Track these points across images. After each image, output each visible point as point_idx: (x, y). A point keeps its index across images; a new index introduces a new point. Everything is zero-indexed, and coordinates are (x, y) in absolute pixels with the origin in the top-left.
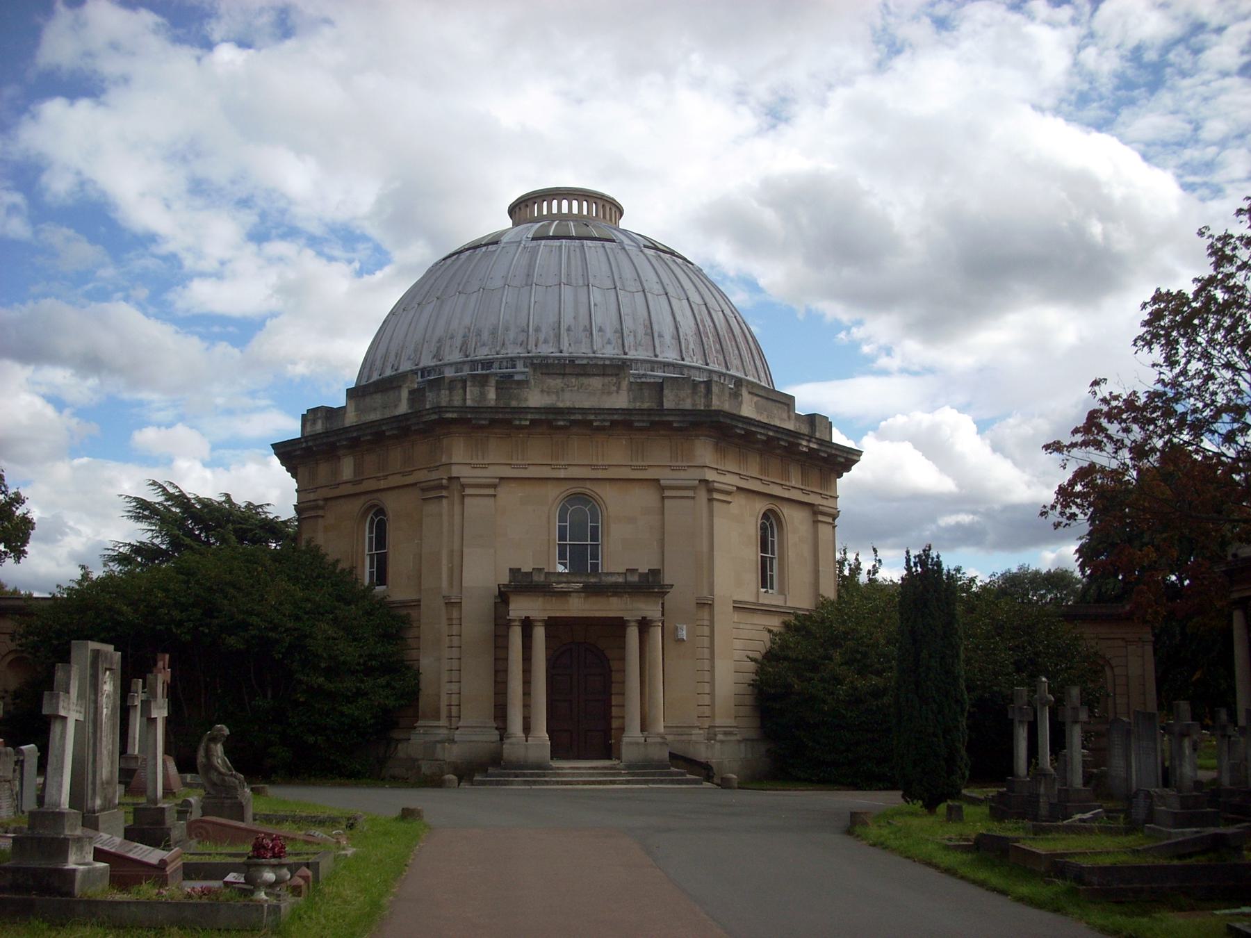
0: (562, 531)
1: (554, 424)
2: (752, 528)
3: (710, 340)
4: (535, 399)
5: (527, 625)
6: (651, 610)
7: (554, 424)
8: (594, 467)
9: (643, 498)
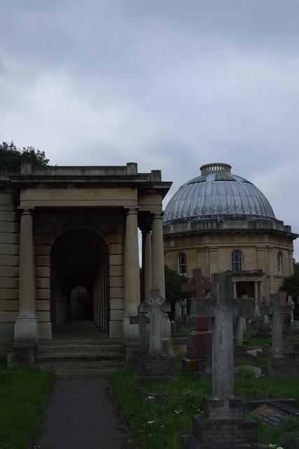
1: (231, 233)
3: (263, 208)
4: (225, 226)
6: (260, 279)
7: (231, 233)
8: (241, 243)
9: (253, 251)
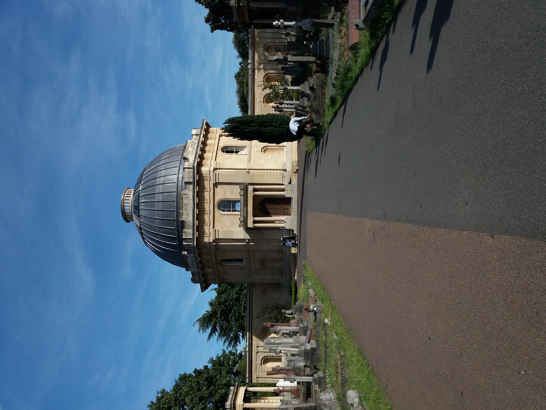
0: (228, 211)
2: (228, 155)
5: (255, 222)
6: (250, 188)
